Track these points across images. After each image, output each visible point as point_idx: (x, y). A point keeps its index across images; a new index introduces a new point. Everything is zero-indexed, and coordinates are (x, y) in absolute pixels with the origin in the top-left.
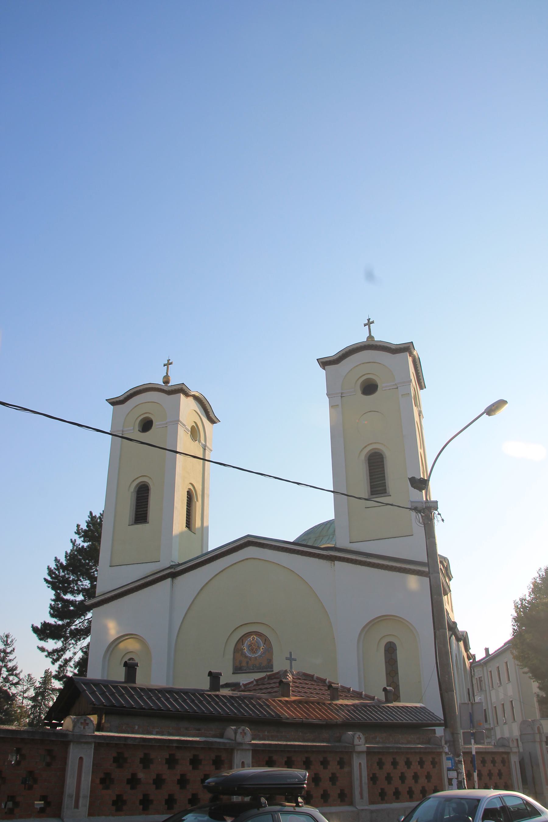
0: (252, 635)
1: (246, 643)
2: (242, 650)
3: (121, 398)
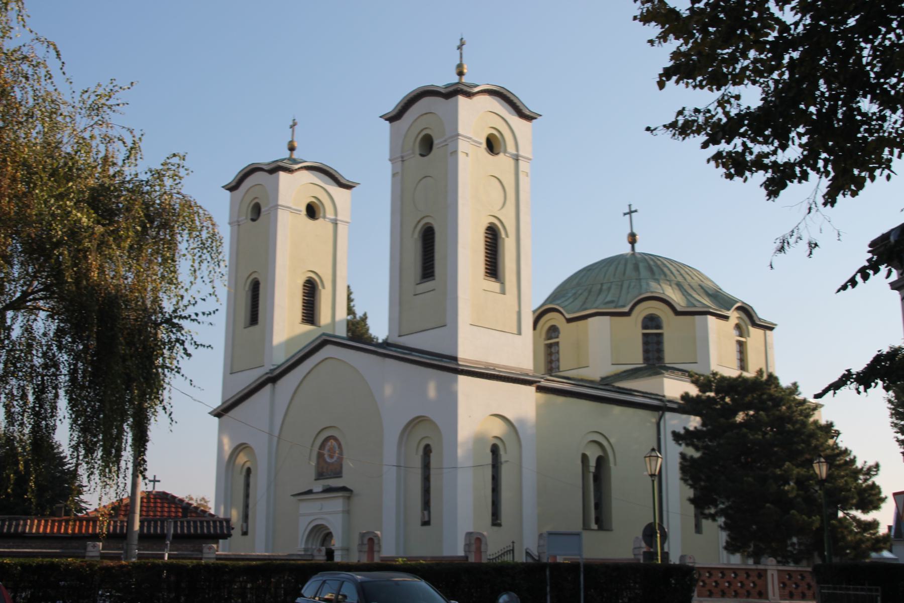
1: (327, 448)
2: (323, 455)
3: (234, 184)
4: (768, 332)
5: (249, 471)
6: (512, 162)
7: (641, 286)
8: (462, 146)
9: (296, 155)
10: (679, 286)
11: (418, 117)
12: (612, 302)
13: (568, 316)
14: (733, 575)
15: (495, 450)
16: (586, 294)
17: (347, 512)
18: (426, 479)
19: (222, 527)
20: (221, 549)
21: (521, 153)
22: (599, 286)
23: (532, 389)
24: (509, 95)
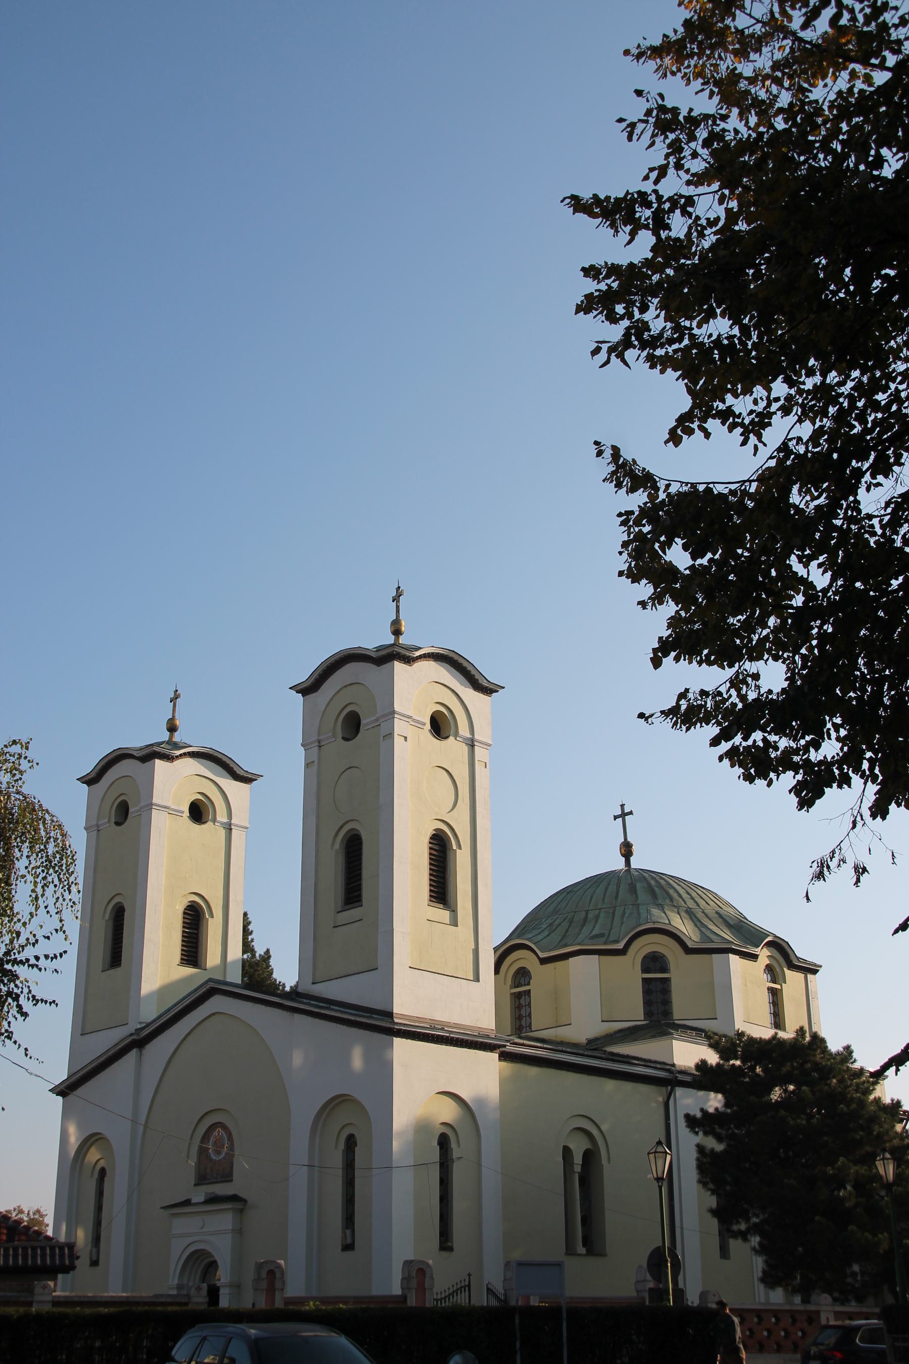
0: (217, 1127)
1: (212, 1140)
3: (93, 775)
4: (810, 976)
5: (103, 1172)
6: (466, 749)
7: (639, 914)
8: (400, 727)
9: (177, 737)
10: (690, 913)
11: (342, 689)
12: (602, 935)
13: (542, 955)
14: (773, 1320)
15: (444, 1142)
16: (565, 924)
17: (239, 1231)
18: (349, 1183)
19: (62, 1255)
20: (60, 1288)
21: (477, 737)
22: (584, 914)
23: (495, 1056)
24: (461, 661)
